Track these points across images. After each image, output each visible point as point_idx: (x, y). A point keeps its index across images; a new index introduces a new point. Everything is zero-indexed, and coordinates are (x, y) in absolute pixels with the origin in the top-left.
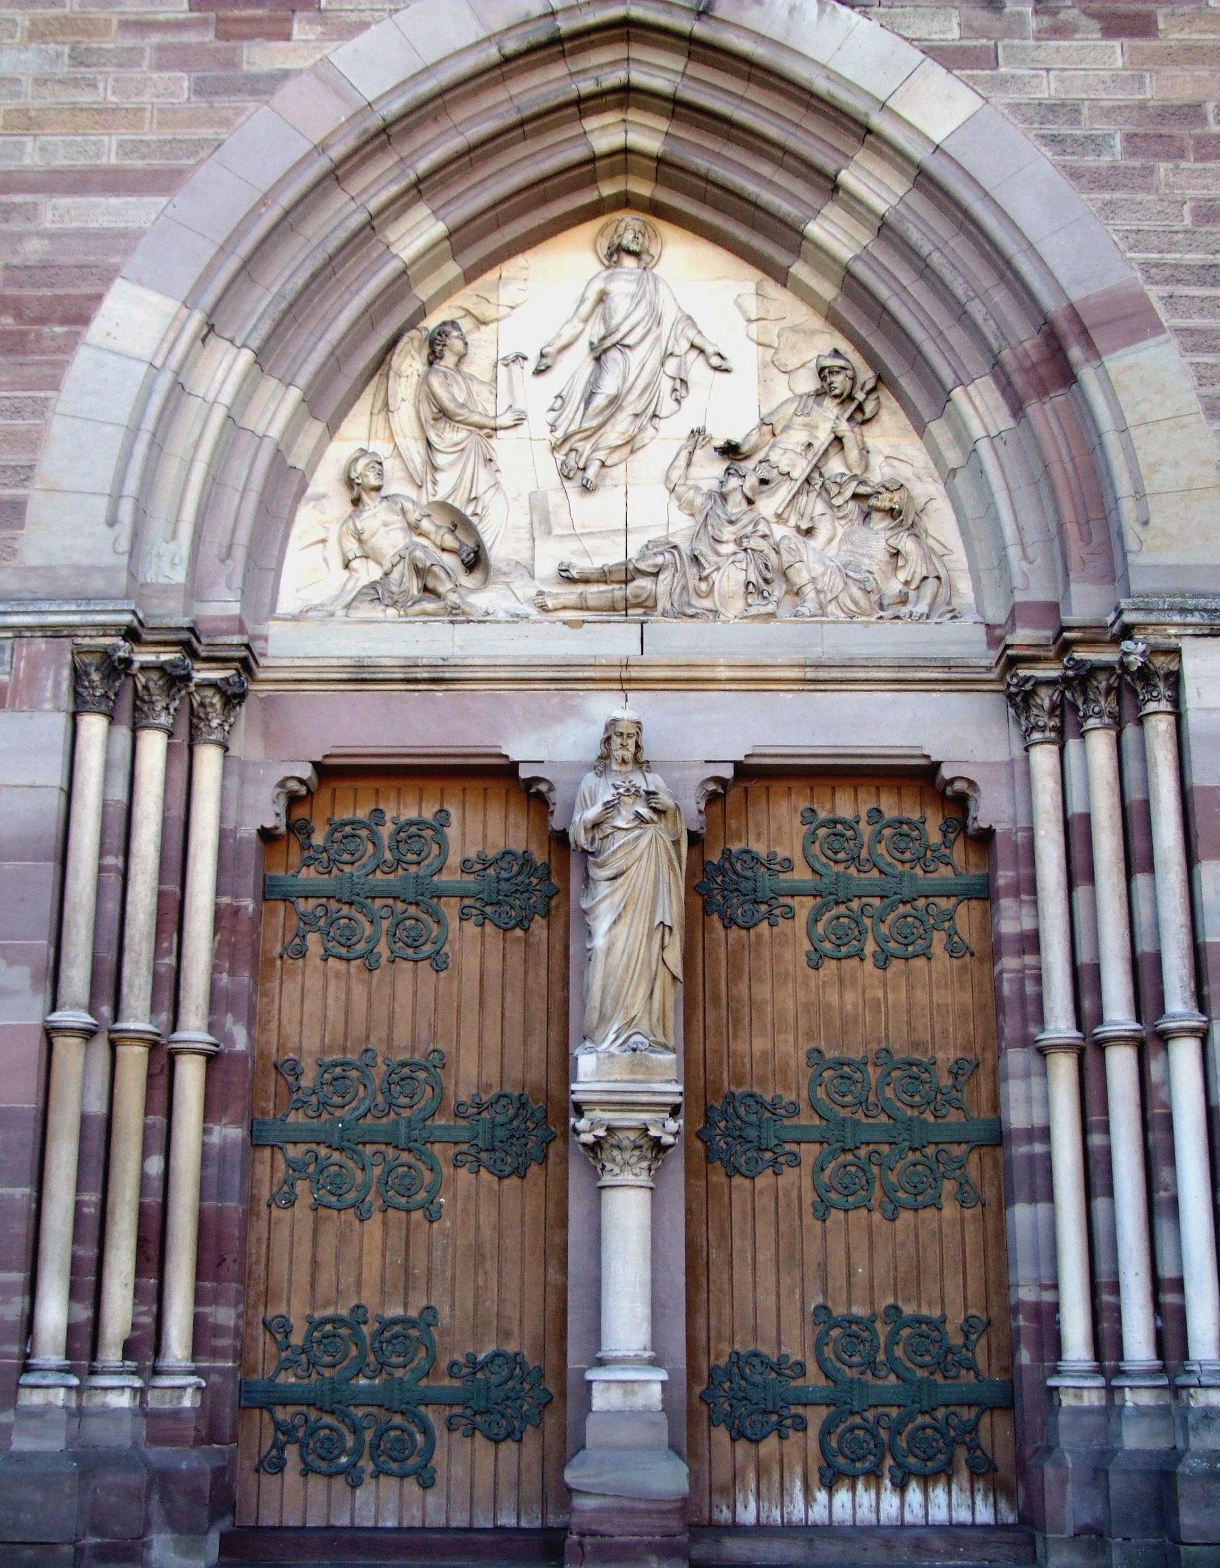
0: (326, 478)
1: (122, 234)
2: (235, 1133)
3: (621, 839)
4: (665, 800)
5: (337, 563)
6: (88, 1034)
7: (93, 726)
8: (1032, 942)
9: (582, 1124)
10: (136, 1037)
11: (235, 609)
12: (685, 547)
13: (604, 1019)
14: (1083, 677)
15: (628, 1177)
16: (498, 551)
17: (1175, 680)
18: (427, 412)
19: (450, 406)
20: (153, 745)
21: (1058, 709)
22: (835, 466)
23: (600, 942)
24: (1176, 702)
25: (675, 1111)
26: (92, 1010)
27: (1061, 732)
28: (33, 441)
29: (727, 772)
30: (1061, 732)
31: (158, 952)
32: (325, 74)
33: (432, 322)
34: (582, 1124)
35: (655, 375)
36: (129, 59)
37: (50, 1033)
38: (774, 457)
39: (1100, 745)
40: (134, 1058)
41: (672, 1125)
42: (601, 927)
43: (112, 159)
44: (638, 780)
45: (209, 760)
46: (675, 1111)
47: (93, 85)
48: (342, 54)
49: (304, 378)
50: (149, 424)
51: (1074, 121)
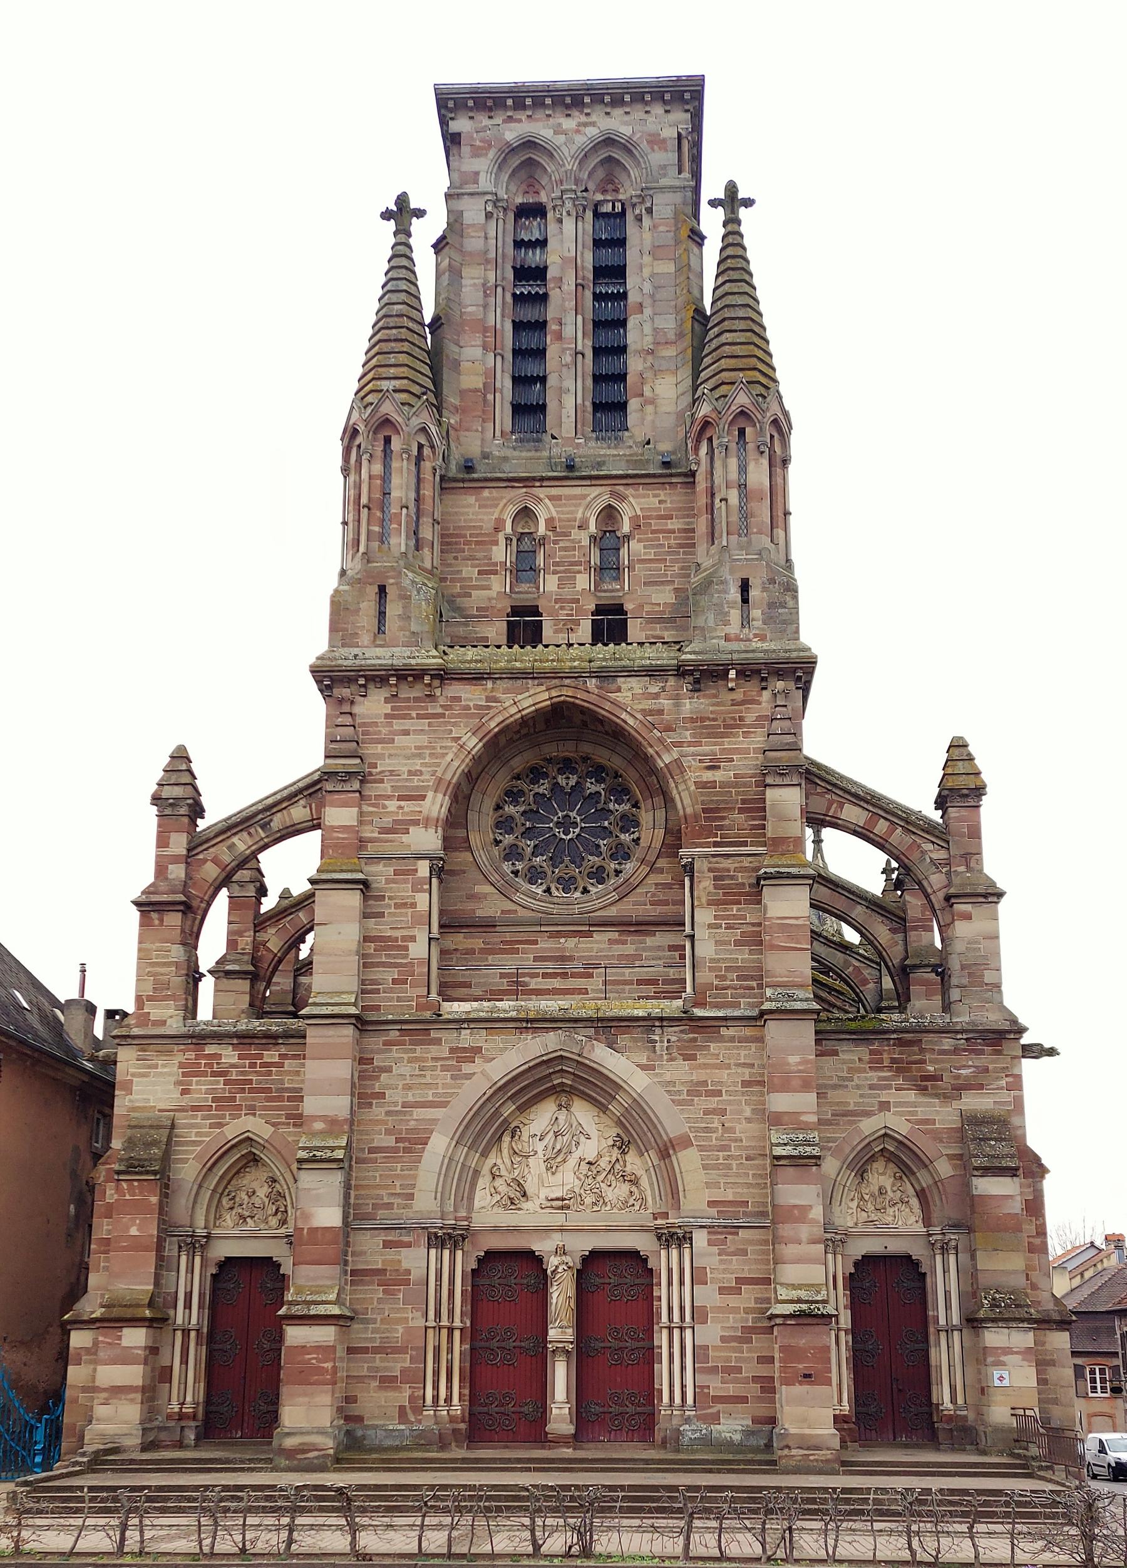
0: (485, 1170)
1: (434, 1120)
2: (468, 1346)
3: (559, 1275)
4: (571, 1264)
5: (489, 1195)
6: (434, 1327)
7: (433, 1252)
8: (659, 1299)
9: (550, 1346)
10: (444, 1327)
11: (465, 1214)
12: (577, 1192)
13: (556, 1320)
14: (672, 1235)
15: (561, 1359)
16: (530, 1188)
17: (691, 1239)
18: (511, 1152)
19: (517, 1151)
20: (446, 1253)
21: (667, 1240)
22: (617, 1166)
23: (554, 1301)
24: (691, 1244)
25: (572, 1343)
26: (435, 1321)
27: (668, 1246)
28: (415, 1177)
29: (587, 1253)
30: (668, 1246)
31: (449, 1304)
32: (483, 1073)
33: (512, 1126)
34: (550, 1346)
35: (571, 1141)
36: (434, 1068)
37: (426, 1328)
38: (601, 1164)
39: (674, 1253)
40: (444, 1332)
41: (571, 1346)
42: (555, 1296)
43: (430, 1098)
44: (564, 1258)
45: (459, 1253)
46: (572, 1343)
47: (425, 1076)
48: (488, 1067)
49: (479, 1151)
50: (443, 1172)
51: (675, 1087)
